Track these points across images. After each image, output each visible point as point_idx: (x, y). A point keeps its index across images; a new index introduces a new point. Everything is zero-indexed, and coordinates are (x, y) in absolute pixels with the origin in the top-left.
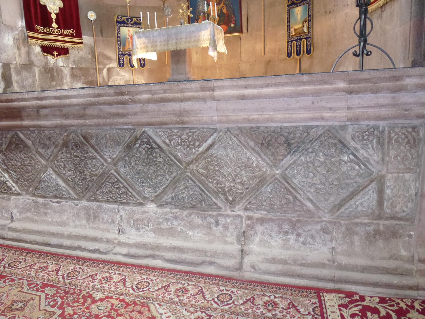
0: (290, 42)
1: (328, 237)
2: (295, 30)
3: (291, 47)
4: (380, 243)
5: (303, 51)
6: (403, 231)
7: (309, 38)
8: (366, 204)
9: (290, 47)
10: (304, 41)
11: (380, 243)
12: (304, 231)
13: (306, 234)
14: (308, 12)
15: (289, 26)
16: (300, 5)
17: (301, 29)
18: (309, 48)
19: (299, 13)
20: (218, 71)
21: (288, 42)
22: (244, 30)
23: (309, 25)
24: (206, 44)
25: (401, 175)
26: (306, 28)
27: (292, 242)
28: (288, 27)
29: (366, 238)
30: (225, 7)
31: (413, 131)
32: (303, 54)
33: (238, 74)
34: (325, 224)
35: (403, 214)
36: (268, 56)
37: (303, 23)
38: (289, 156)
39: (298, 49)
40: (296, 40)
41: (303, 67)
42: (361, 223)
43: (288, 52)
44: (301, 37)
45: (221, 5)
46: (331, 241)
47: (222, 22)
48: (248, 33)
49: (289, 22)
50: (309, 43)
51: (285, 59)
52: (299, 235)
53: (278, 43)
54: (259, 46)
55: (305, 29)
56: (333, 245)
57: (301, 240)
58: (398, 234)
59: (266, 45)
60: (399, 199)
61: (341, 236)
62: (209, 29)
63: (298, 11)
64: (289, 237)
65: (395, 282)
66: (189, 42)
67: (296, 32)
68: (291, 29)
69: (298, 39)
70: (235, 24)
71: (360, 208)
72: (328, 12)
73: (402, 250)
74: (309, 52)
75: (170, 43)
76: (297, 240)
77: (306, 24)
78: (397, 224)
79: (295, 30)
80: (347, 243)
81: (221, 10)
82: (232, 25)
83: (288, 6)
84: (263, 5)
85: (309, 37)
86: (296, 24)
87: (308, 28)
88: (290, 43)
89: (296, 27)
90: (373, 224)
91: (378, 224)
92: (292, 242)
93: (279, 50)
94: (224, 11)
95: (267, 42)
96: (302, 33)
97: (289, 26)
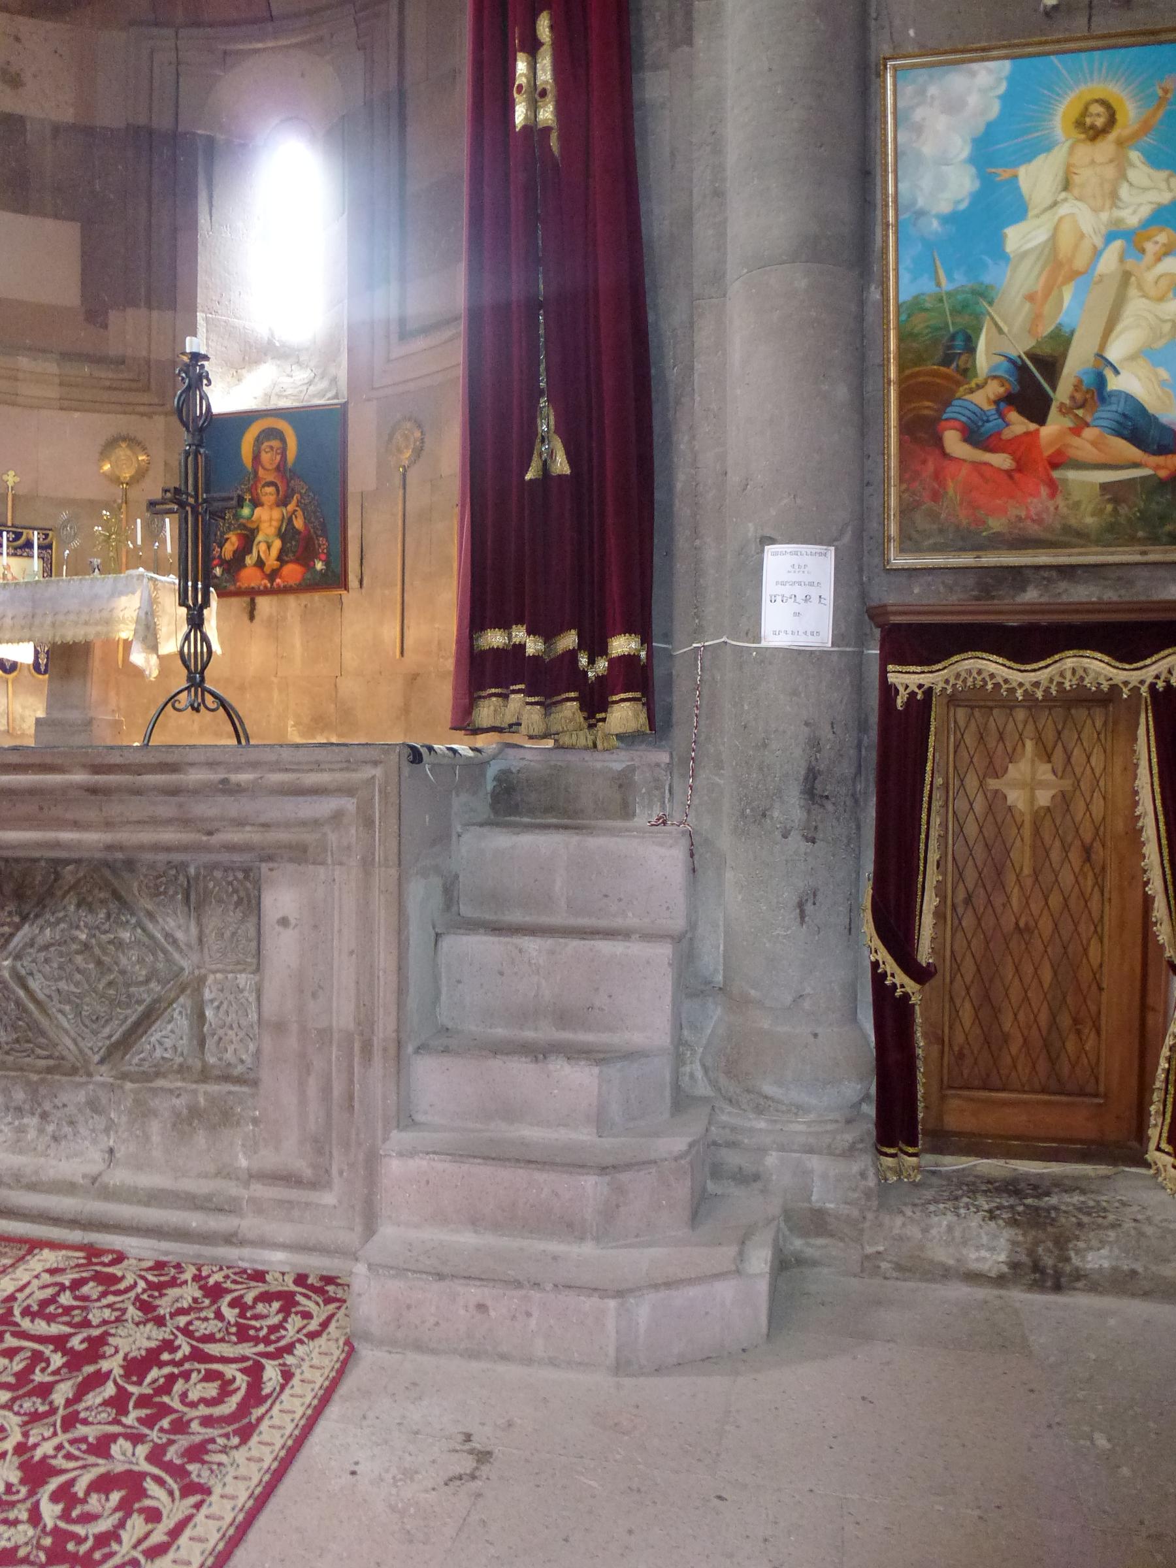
1: (100, 1122)
4: (201, 1139)
6: (243, 1110)
8: (168, 1043)
11: (201, 1139)
12: (56, 1107)
13: (59, 1115)
20: (276, 694)
22: (353, 581)
24: (126, 633)
25: (230, 976)
27: (32, 1134)
29: (174, 1125)
30: (299, 513)
31: (246, 877)
33: (333, 706)
34: (94, 1091)
35: (240, 1069)
38: (27, 926)
42: (162, 1089)
45: (290, 507)
46: (107, 1130)
47: (291, 555)
48: (364, 590)
52: (44, 1116)
53: (437, 626)
54: (390, 632)
56: (111, 1143)
57: (50, 1128)
58: (234, 1115)
60: (230, 1032)
61: (124, 1119)
62: (138, 594)
64: (25, 1121)
65: (194, 1224)
66: (86, 623)
70: (327, 563)
71: (158, 1053)
73: (240, 1155)
75: (37, 622)
76: (41, 1131)
78: (229, 1093)
80: (138, 1137)
81: (290, 520)
82: (319, 566)
90: (186, 1091)
91: (195, 1092)
92: (32, 1134)
94: (299, 523)
95: (410, 621)
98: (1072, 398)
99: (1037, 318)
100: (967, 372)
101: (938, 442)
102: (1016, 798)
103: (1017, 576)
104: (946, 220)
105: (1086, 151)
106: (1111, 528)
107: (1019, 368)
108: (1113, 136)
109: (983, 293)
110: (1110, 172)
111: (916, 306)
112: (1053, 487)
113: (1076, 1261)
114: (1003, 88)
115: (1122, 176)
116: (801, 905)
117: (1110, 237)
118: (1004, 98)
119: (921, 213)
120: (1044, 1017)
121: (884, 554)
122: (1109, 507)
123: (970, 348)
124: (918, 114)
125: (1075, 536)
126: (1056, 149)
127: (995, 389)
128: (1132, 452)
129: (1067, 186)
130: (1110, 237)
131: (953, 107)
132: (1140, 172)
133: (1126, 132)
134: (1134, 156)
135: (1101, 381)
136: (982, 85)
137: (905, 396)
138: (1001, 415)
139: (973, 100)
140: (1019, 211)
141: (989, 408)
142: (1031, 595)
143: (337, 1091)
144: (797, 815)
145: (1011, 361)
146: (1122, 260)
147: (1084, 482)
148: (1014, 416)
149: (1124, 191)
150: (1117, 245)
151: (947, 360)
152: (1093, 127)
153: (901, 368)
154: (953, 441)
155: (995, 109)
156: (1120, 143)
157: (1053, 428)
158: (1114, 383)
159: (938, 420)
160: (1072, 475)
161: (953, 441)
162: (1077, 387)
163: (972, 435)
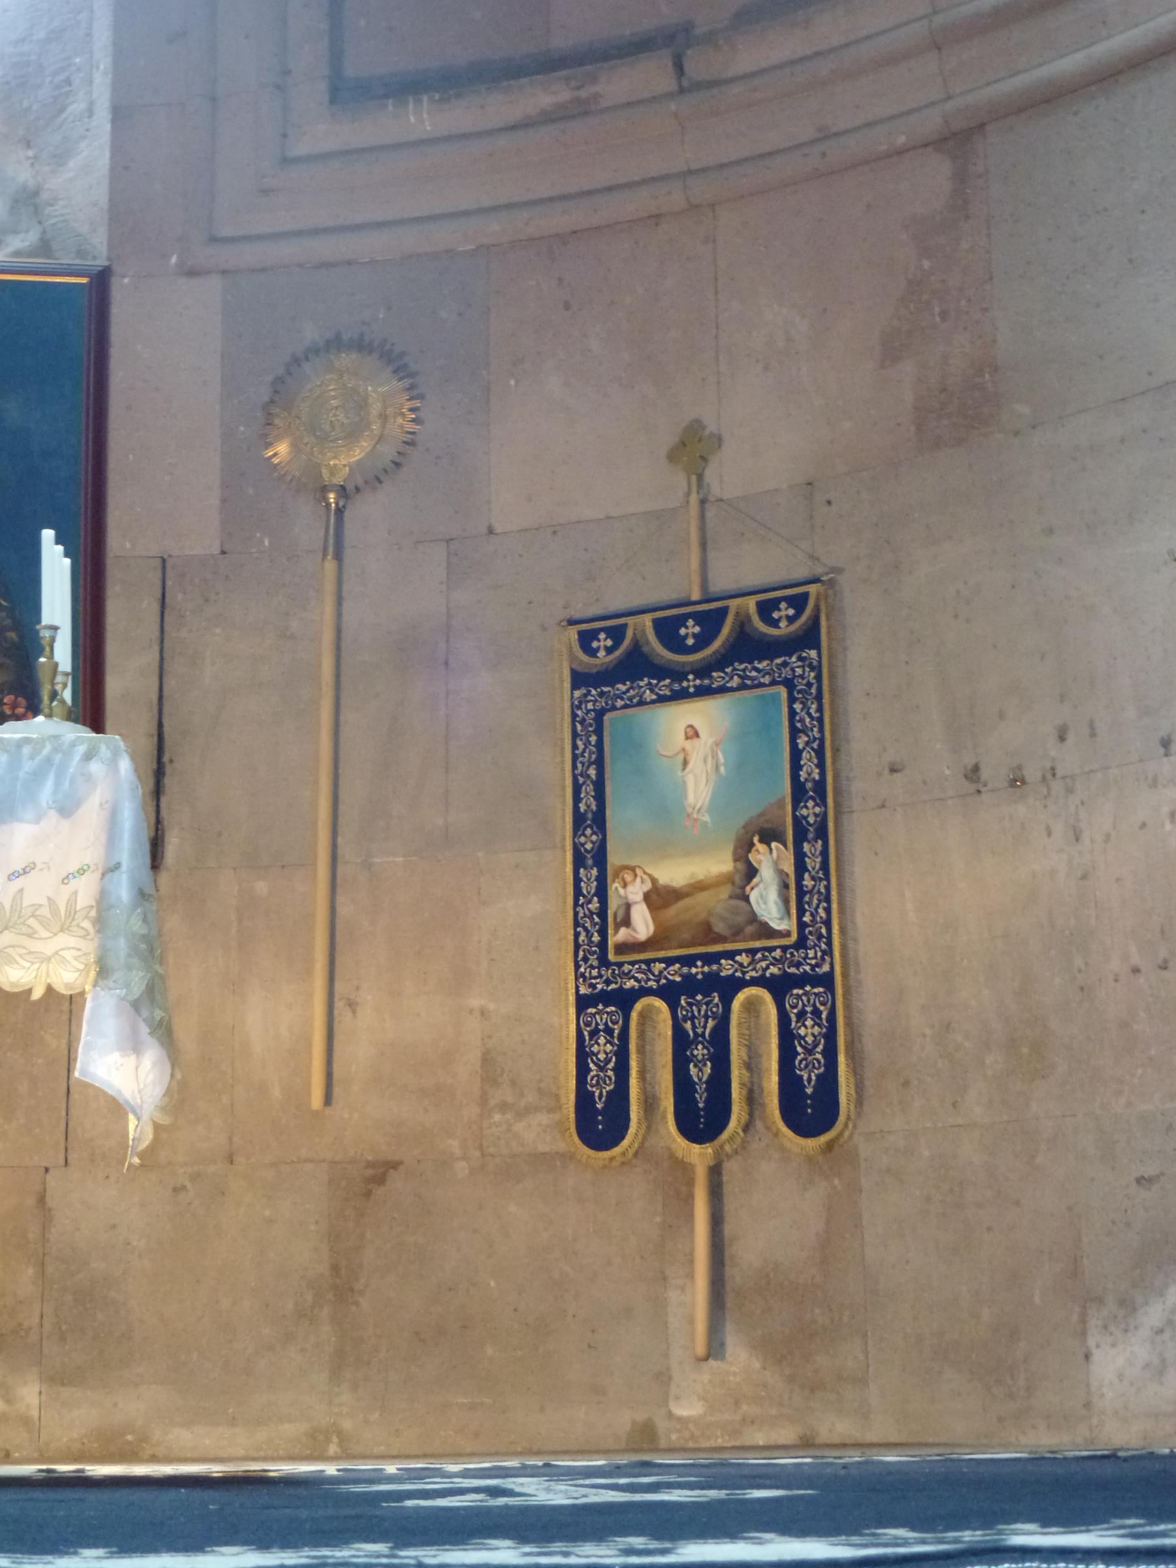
0: (605, 998)
2: (659, 898)
3: (622, 1054)
5: (753, 1099)
7: (816, 980)
9: (603, 1048)
10: (751, 1007)
14: (796, 754)
15: (593, 862)
16: (704, 692)
17: (725, 892)
18: (809, 1077)
19: (699, 751)
21: (583, 1003)
23: (800, 867)
26: (773, 895)
28: (579, 861)
32: (746, 1128)
36: (366, 1118)
37: (743, 848)
39: (700, 1073)
40: (669, 993)
41: (749, 1250)
43: (584, 1099)
44: (727, 968)
49: (591, 820)
50: (808, 1031)
51: (542, 1160)
53: (475, 1002)
55: (768, 902)
59: (352, 1005)
63: (693, 733)
67: (672, 913)
68: (614, 887)
69: (690, 986)
74: (810, 1108)
77: (771, 862)
79: (659, 898)
83: (579, 679)
84: (328, 637)
85: (804, 976)
86: (664, 849)
87: (798, 893)
88: (603, 1015)
89: (674, 873)
93: (490, 1067)
96: (737, 933)
97: (593, 862)
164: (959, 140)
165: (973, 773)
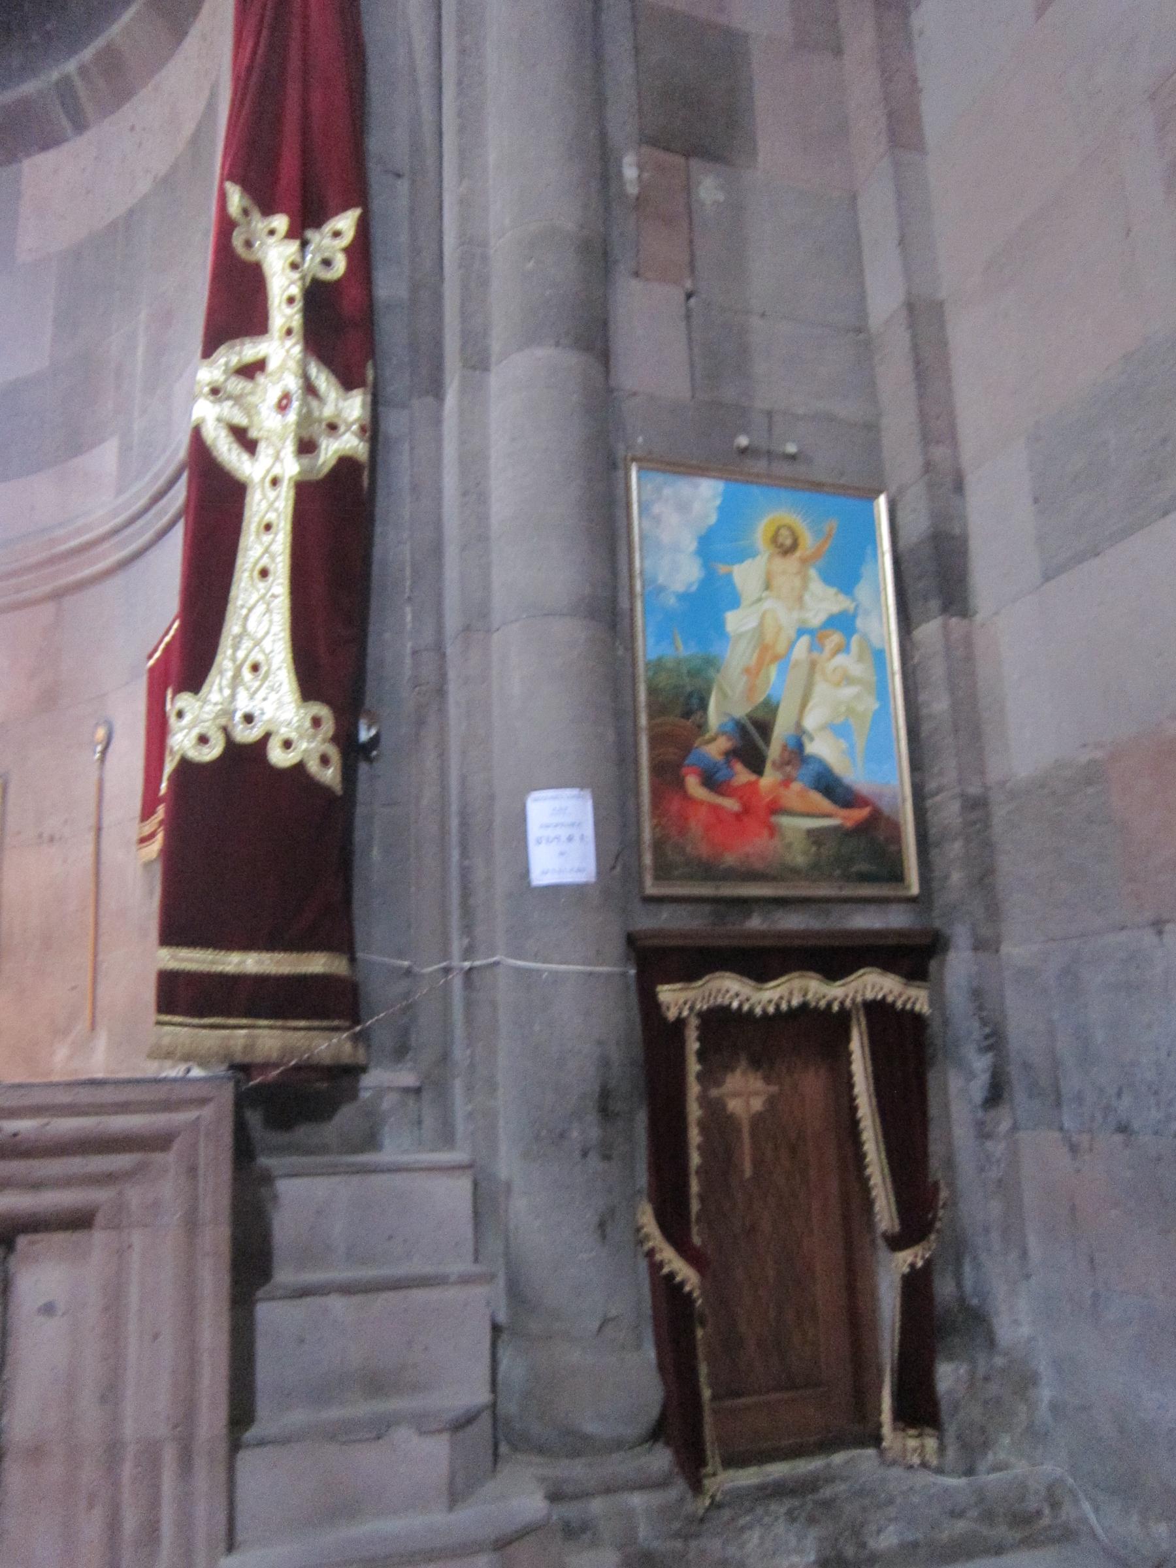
72: (46, 835)
98: (781, 756)
99: (751, 689)
100: (702, 727)
101: (680, 784)
102: (734, 1105)
103: (745, 905)
104: (683, 597)
105: (780, 564)
106: (815, 866)
107: (741, 728)
108: (798, 554)
109: (711, 662)
110: (797, 582)
111: (657, 666)
112: (773, 830)
113: (872, 1544)
114: (718, 502)
115: (805, 587)
116: (602, 1225)
117: (801, 632)
118: (721, 509)
119: (661, 589)
120: (772, 1314)
121: (641, 883)
122: (814, 849)
123: (703, 705)
124: (656, 509)
125: (788, 873)
126: (759, 557)
127: (723, 744)
128: (825, 804)
129: (768, 586)
130: (801, 632)
131: (683, 507)
132: (817, 586)
133: (808, 553)
134: (813, 573)
135: (800, 746)
136: (706, 494)
137: (654, 741)
138: (728, 762)
139: (697, 506)
140: (735, 602)
141: (719, 758)
142: (755, 923)
143: (130, 1523)
144: (595, 1133)
145: (733, 719)
146: (811, 649)
147: (795, 825)
148: (739, 767)
149: (807, 597)
150: (804, 641)
151: (687, 715)
152: (782, 545)
153: (651, 717)
154: (693, 785)
155: (713, 519)
156: (804, 561)
157: (769, 779)
158: (811, 748)
159: (679, 766)
160: (785, 821)
161: (693, 785)
162: (785, 747)
163: (709, 780)
164: (57, 595)
165: (40, 836)
